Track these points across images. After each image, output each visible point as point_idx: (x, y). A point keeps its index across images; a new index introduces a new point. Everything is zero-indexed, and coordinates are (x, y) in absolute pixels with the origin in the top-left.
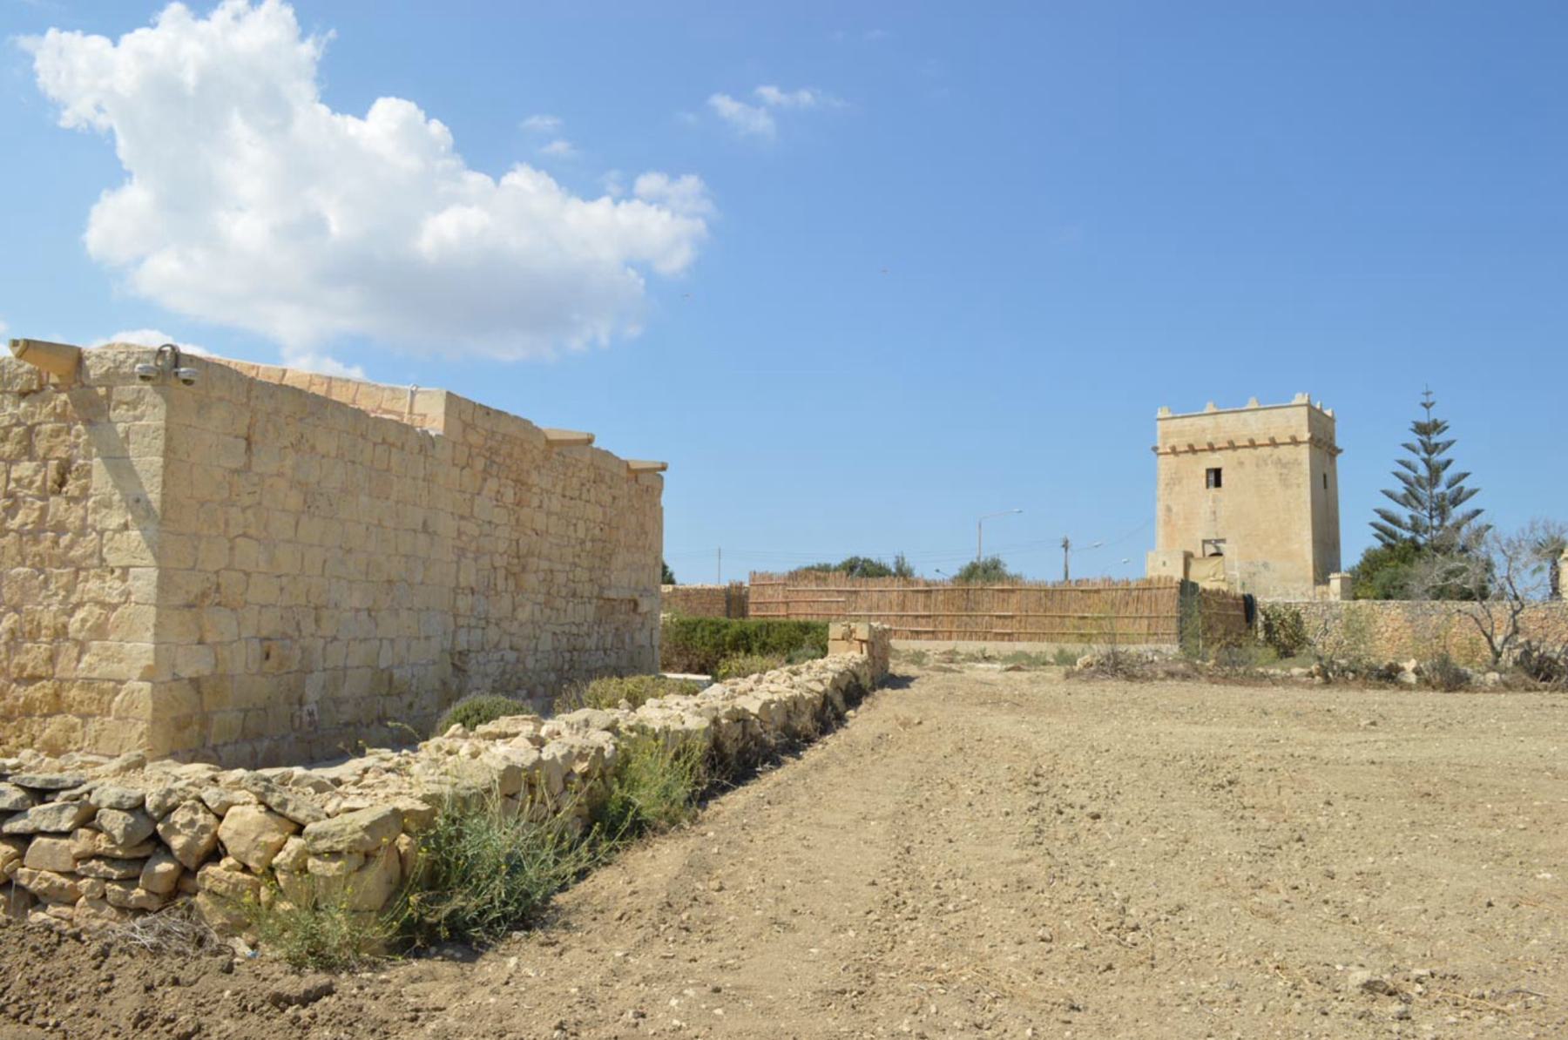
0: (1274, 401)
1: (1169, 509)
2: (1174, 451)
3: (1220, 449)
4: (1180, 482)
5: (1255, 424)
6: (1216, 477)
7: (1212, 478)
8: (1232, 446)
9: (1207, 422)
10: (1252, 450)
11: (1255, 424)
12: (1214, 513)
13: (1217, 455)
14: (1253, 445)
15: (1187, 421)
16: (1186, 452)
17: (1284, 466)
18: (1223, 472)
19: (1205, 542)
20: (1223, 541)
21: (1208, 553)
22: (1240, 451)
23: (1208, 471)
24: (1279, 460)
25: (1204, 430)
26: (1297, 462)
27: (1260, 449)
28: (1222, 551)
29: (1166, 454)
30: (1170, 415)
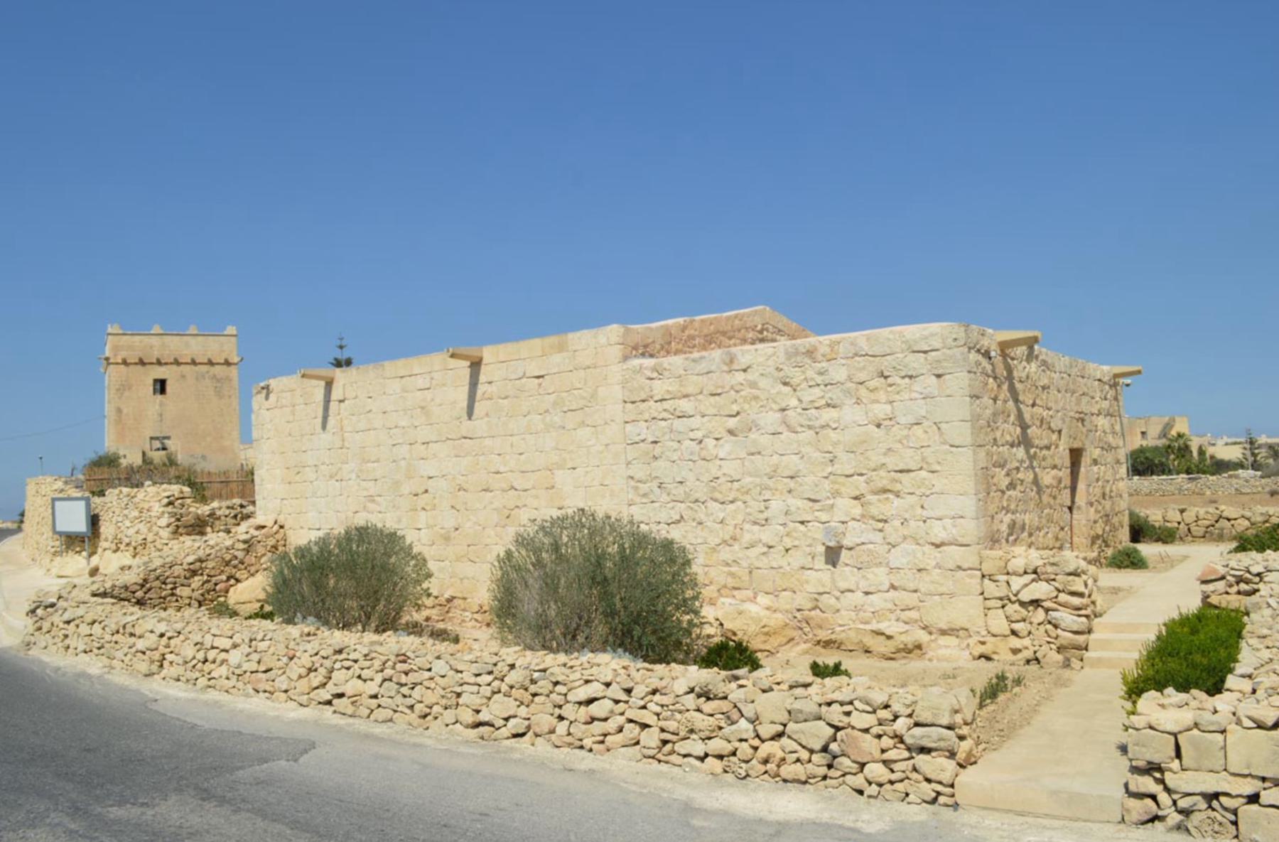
0: (211, 330)
1: (119, 411)
2: (125, 363)
3: (166, 364)
4: (130, 388)
5: (194, 346)
6: (161, 386)
7: (158, 387)
8: (177, 362)
9: (155, 341)
10: (193, 367)
11: (194, 346)
12: (161, 415)
13: (163, 369)
14: (194, 363)
15: (137, 338)
16: (136, 364)
17: (218, 381)
18: (168, 383)
19: (152, 438)
20: (168, 438)
21: (154, 447)
22: (183, 366)
23: (155, 381)
24: (215, 376)
25: (151, 347)
26: (229, 379)
27: (200, 366)
28: (168, 446)
29: (117, 364)
30: (121, 332)
